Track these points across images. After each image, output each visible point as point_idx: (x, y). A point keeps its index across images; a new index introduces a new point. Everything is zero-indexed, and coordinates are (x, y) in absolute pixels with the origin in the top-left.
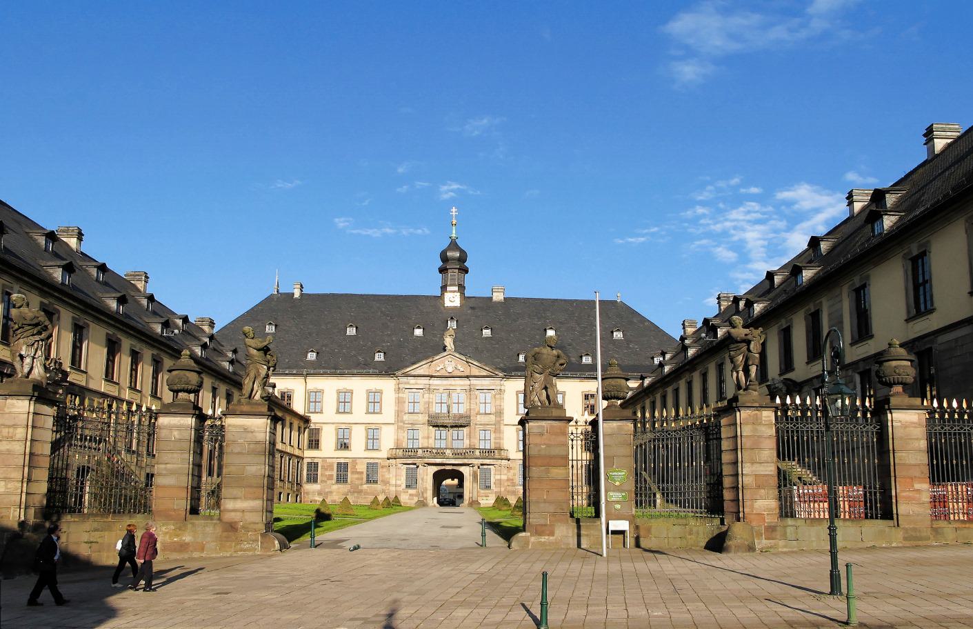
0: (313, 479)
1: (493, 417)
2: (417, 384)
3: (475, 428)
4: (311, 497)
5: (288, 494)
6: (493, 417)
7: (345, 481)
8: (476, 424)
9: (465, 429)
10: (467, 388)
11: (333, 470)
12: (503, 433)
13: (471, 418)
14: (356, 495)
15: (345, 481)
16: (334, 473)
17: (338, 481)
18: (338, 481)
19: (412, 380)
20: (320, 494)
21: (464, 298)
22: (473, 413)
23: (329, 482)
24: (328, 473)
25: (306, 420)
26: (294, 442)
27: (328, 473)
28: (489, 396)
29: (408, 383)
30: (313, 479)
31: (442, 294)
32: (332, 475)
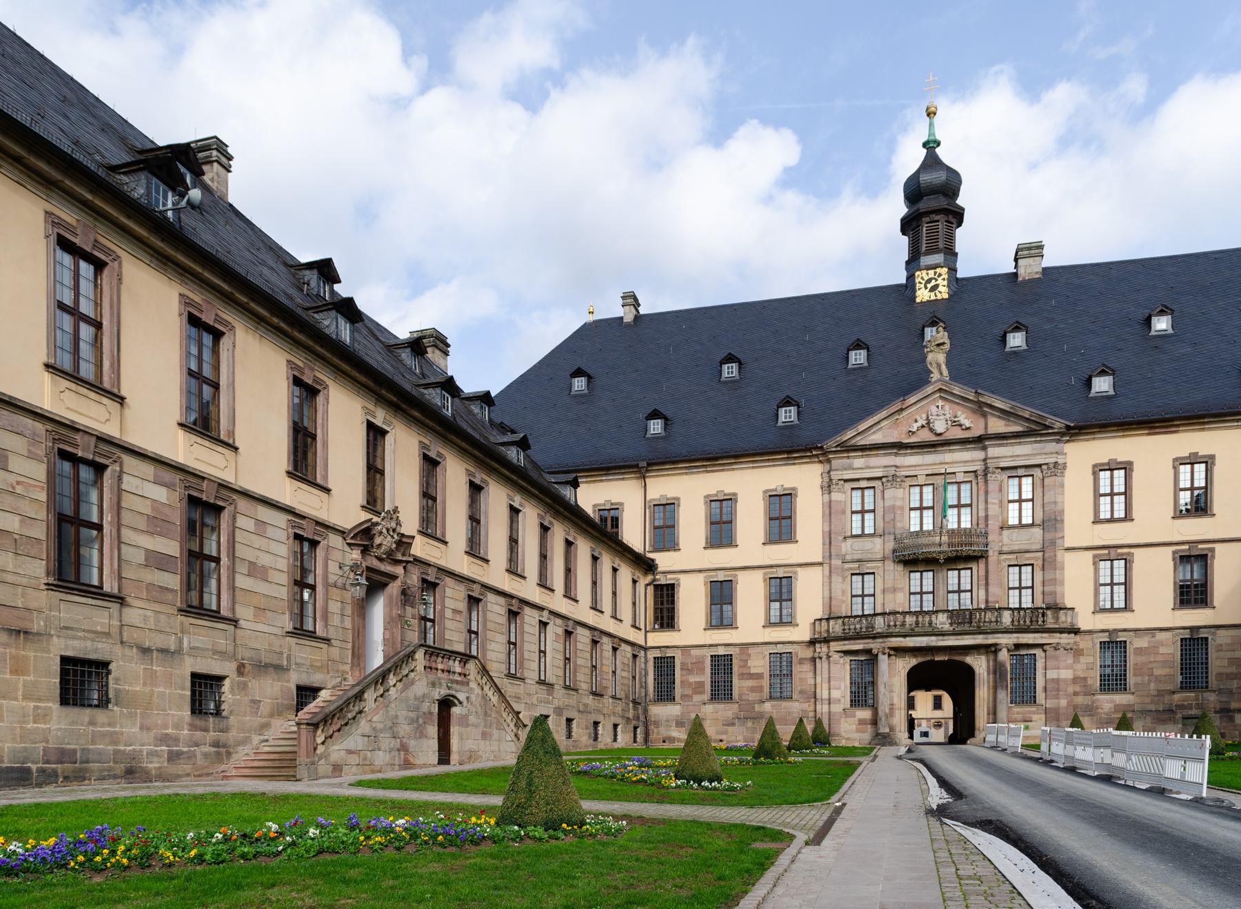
0: (665, 693)
1: (1037, 532)
2: (868, 467)
3: (999, 562)
4: (663, 732)
5: (615, 726)
6: (1037, 532)
7: (728, 696)
8: (1001, 553)
9: (978, 568)
10: (979, 467)
11: (702, 670)
12: (1063, 568)
13: (990, 538)
14: (750, 724)
15: (728, 696)
16: (706, 678)
17: (715, 697)
18: (715, 697)
19: (859, 461)
20: (680, 724)
21: (954, 280)
22: (994, 525)
23: (697, 698)
24: (693, 679)
25: (647, 566)
26: (625, 612)
27: (693, 679)
28: (1026, 483)
29: (851, 468)
30: (665, 693)
31: (911, 277)
32: (701, 684)
